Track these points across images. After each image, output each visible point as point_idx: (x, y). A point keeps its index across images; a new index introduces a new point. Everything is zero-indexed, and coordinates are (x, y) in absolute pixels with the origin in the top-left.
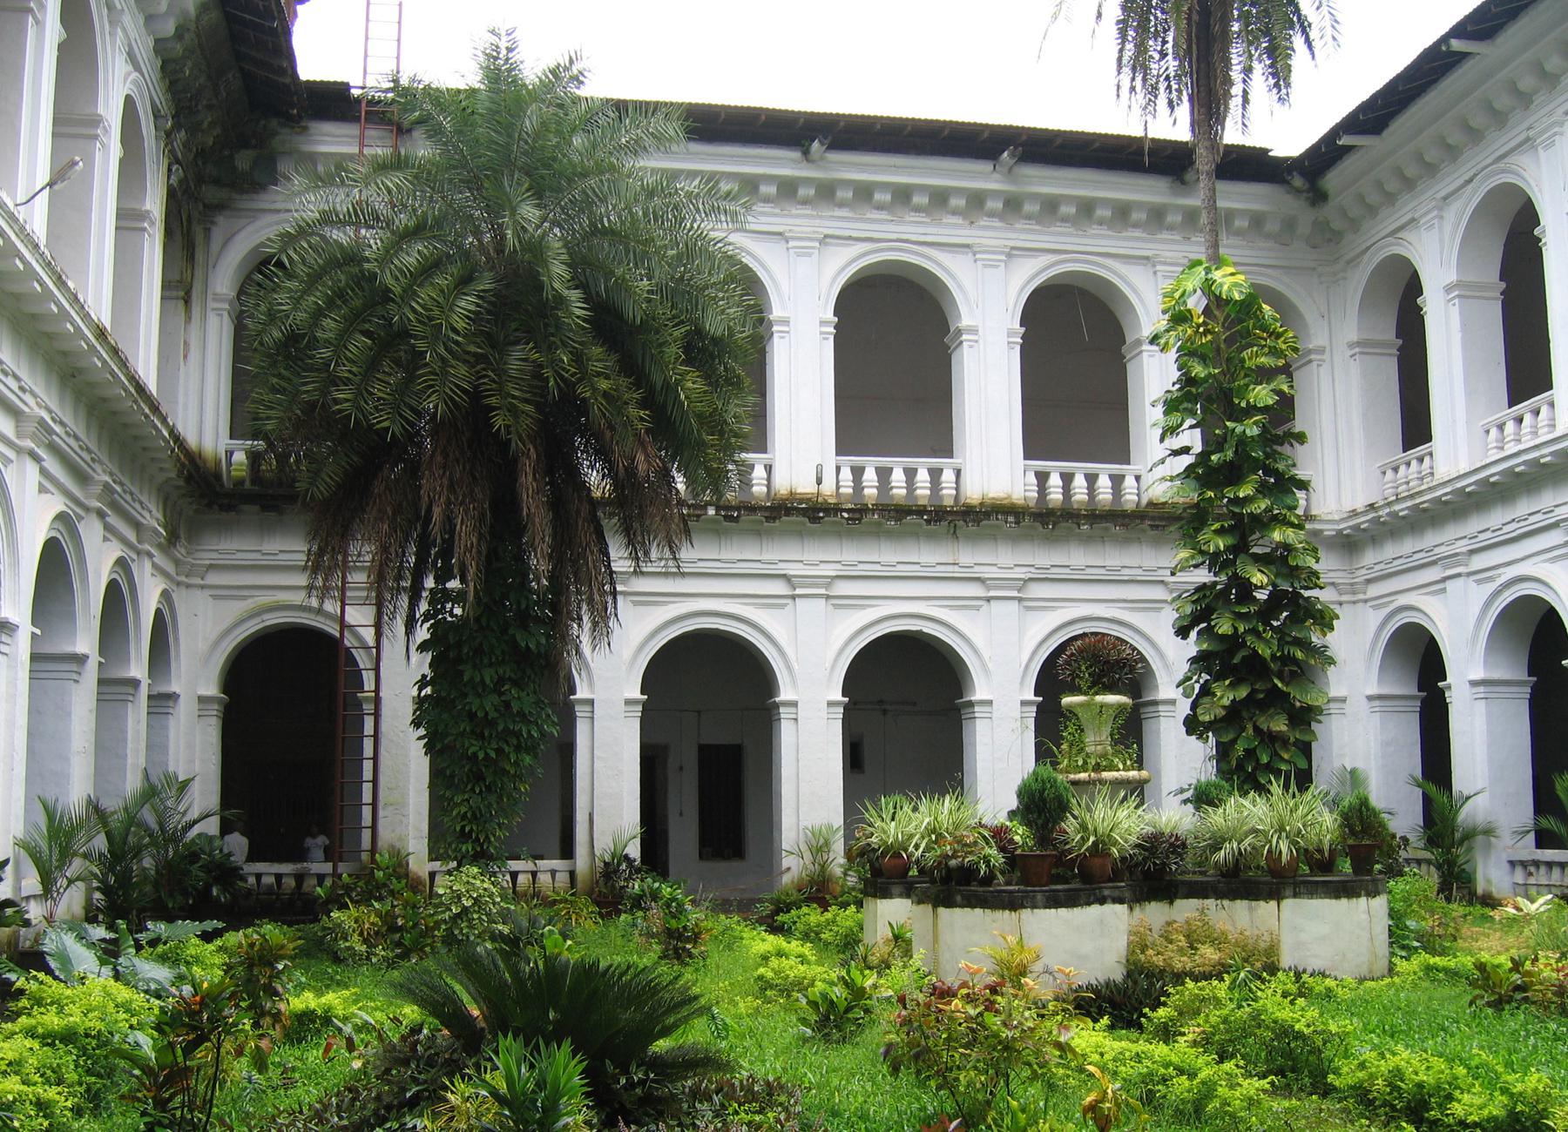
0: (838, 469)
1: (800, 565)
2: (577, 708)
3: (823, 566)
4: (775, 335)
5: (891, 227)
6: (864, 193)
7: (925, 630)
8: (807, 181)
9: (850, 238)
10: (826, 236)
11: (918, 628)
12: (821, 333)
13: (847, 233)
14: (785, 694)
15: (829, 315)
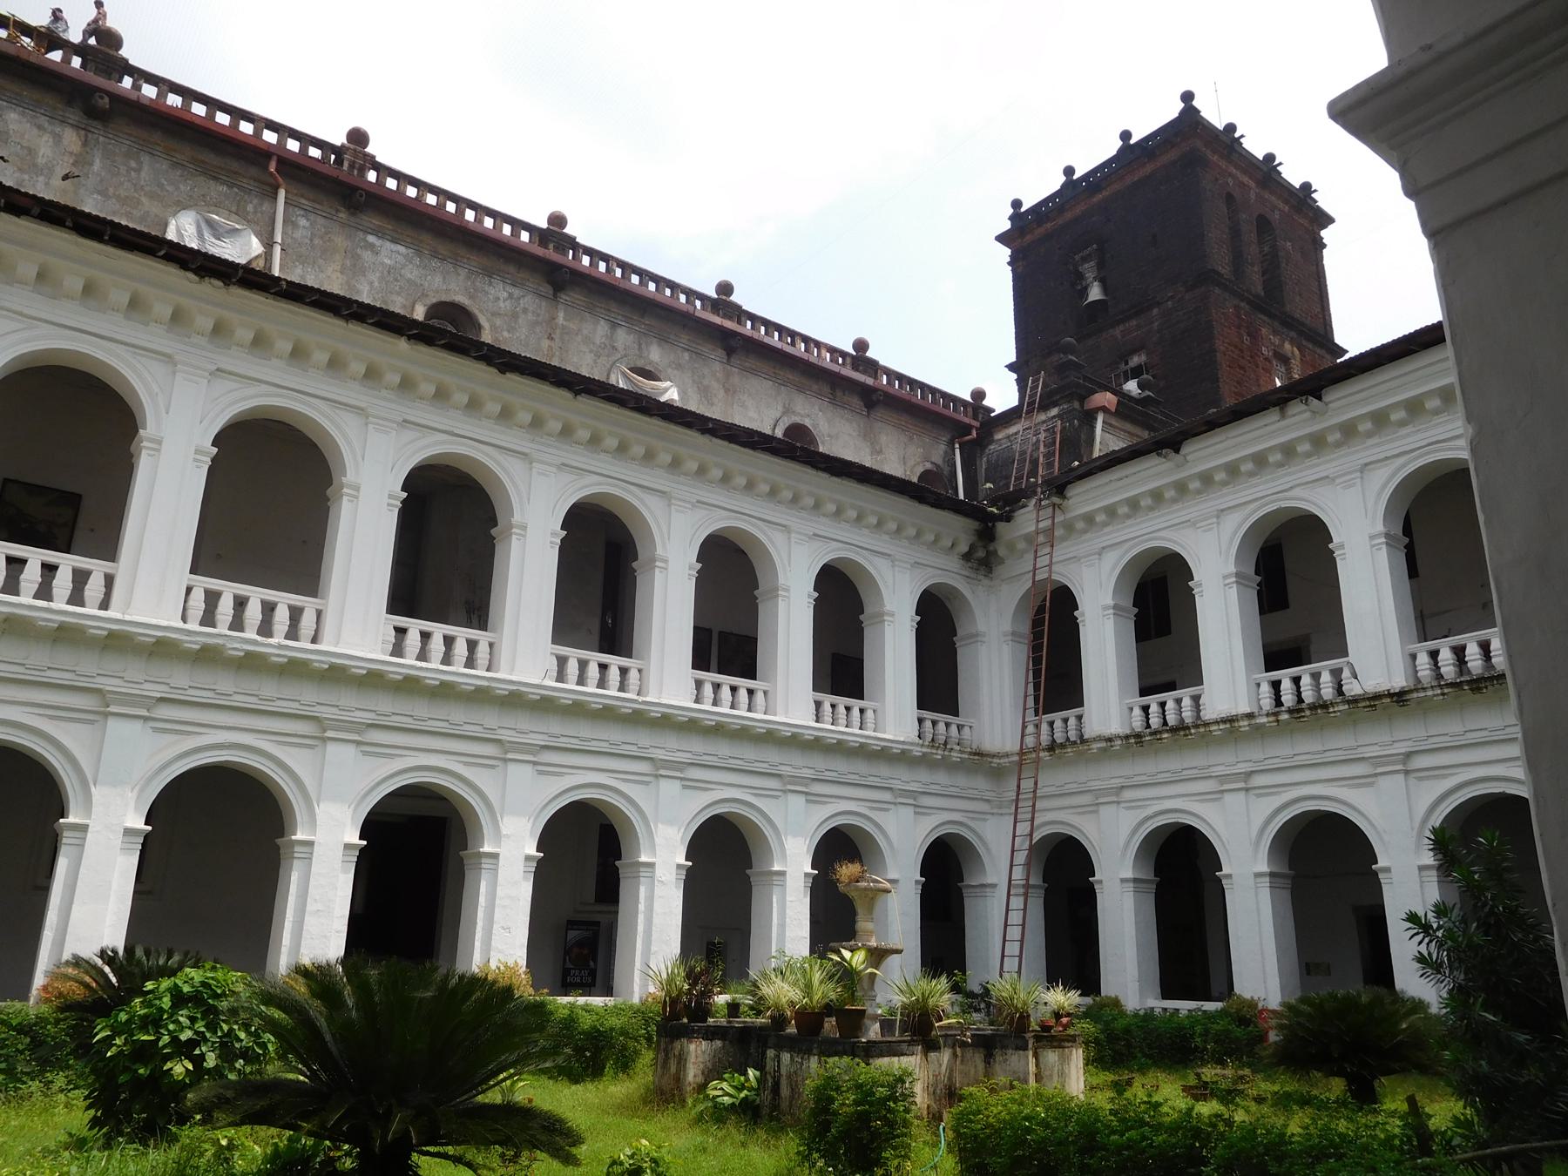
0: (1414, 657)
1: (1377, 748)
2: (1380, 876)
3: (1396, 745)
4: (1337, 559)
5: (1420, 436)
6: (1380, 420)
7: (1508, 791)
8: (1331, 429)
9: (1387, 458)
10: (1366, 465)
11: (1501, 790)
12: (1373, 546)
13: (1382, 456)
14: (1382, 862)
15: (1380, 527)
